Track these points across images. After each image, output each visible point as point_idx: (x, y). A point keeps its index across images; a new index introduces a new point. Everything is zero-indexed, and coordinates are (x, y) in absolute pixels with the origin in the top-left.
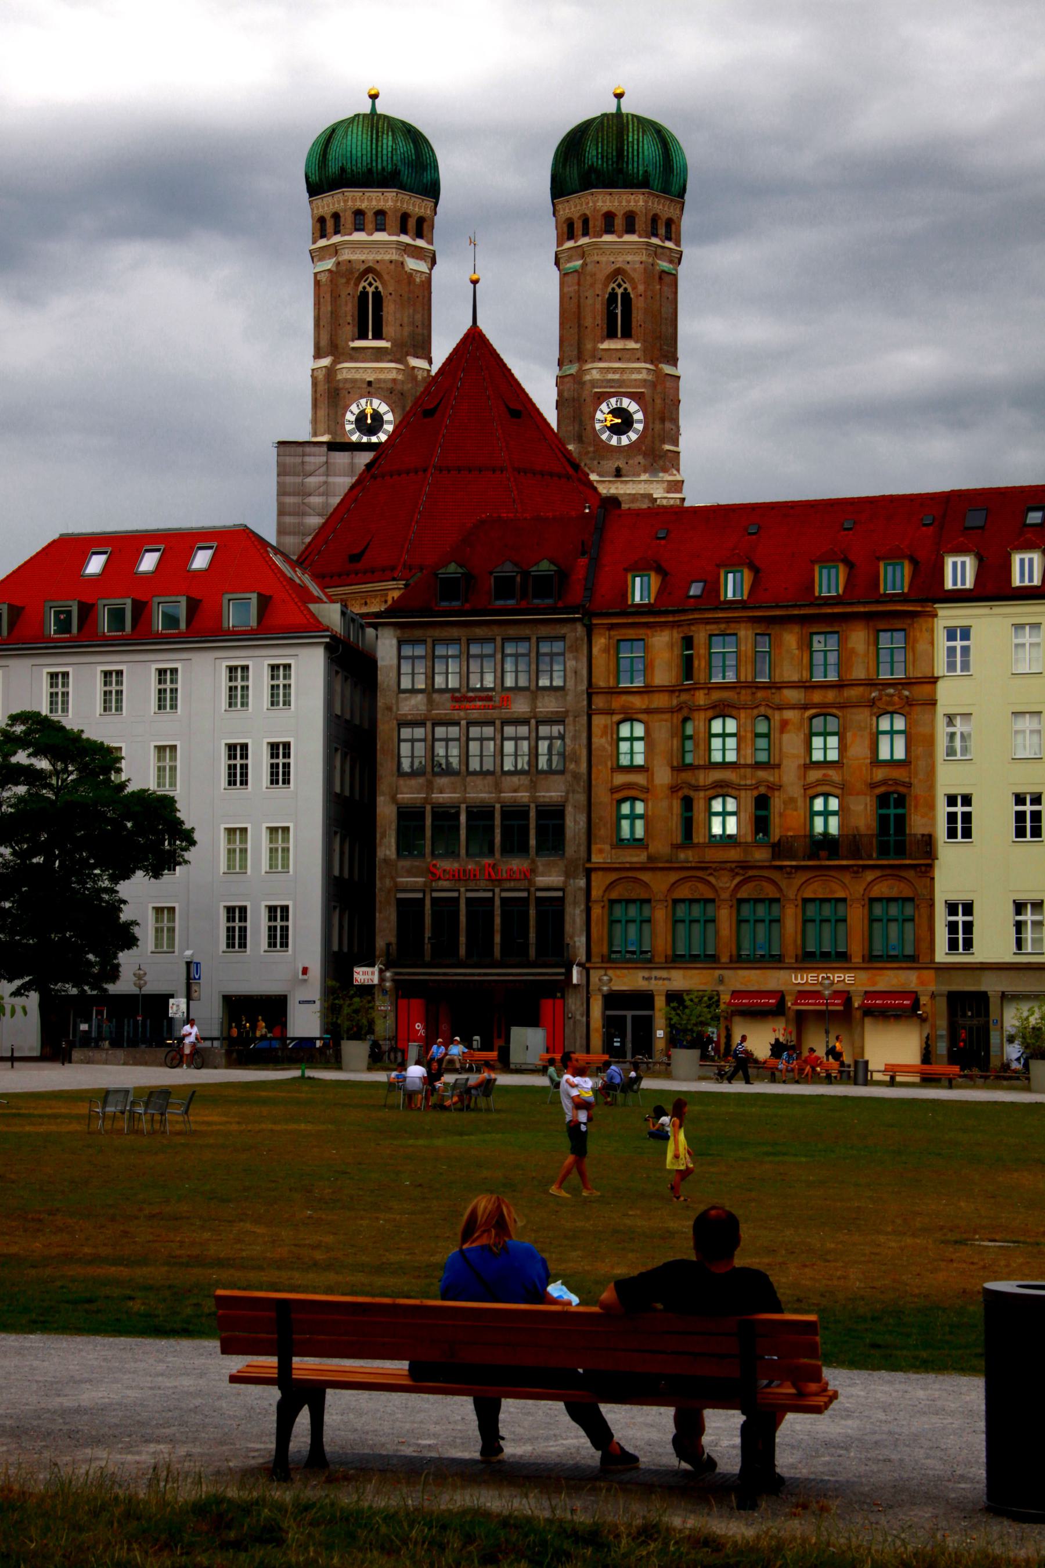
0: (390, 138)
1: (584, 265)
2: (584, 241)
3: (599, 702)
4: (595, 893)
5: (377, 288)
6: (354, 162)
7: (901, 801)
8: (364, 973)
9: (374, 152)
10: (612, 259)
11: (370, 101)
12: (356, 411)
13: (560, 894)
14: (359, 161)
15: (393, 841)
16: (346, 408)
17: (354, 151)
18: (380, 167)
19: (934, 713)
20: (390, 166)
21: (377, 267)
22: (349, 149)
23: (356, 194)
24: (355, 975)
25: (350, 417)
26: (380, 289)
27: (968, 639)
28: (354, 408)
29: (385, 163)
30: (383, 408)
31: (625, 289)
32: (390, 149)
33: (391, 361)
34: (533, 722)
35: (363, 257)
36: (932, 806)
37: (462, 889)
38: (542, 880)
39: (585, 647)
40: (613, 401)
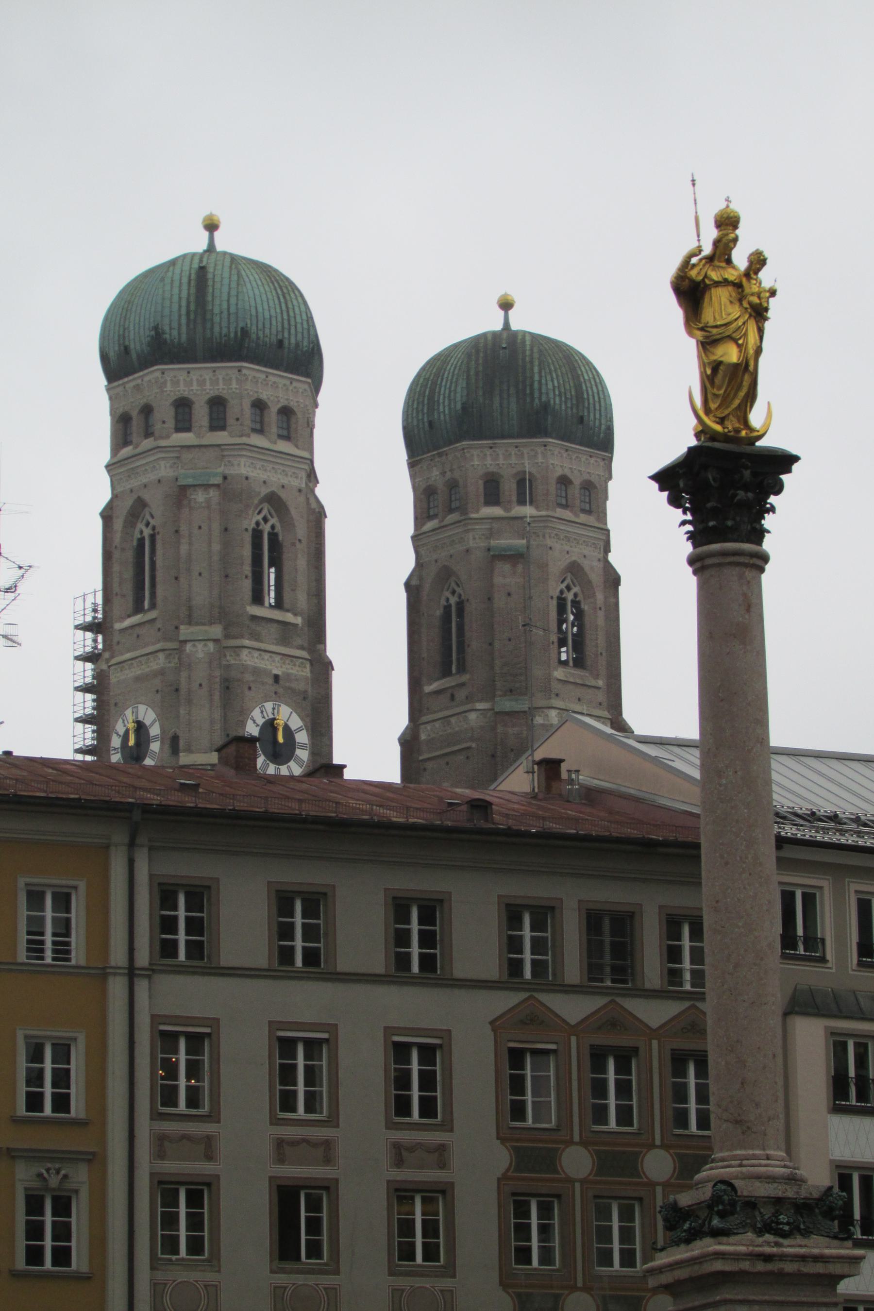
6: (260, 326)
9: (285, 317)
10: (567, 548)
11: (206, 234)
12: (261, 721)
14: (267, 325)
17: (260, 309)
18: (293, 341)
20: (305, 343)
21: (283, 494)
22: (253, 304)
23: (258, 375)
26: (278, 529)
28: (256, 713)
29: (300, 336)
33: (302, 648)
35: (263, 476)
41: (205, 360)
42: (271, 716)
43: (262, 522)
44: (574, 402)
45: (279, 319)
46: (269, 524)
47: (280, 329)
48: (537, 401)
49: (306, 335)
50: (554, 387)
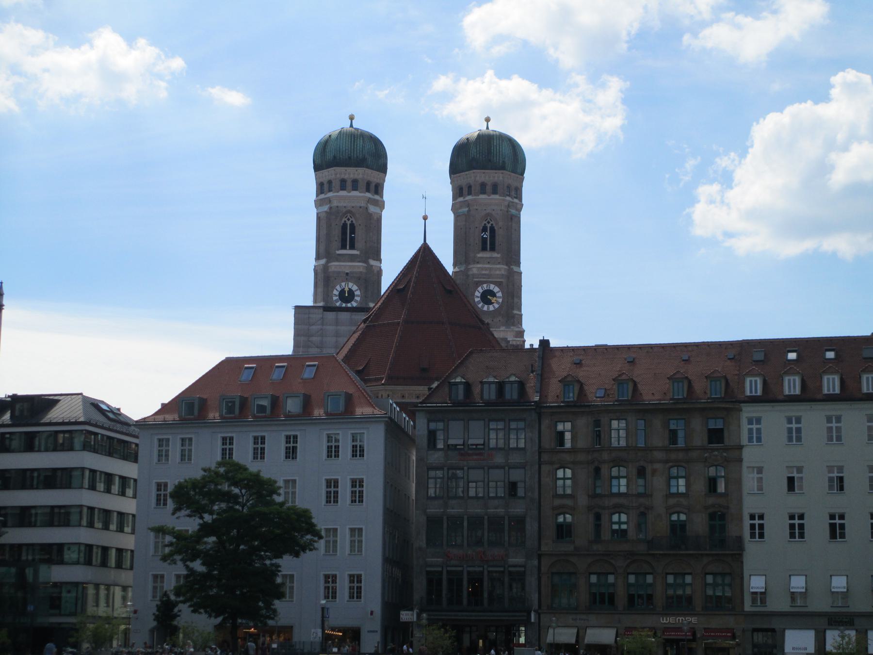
0: (361, 141)
1: (469, 211)
2: (469, 198)
3: (545, 457)
4: (544, 569)
5: (352, 221)
6: (341, 154)
7: (723, 517)
8: (406, 615)
9: (352, 148)
12: (339, 289)
13: (523, 569)
14: (344, 153)
15: (424, 537)
16: (334, 287)
17: (341, 147)
18: (355, 156)
19: (741, 467)
20: (361, 156)
22: (338, 146)
24: (401, 616)
25: (336, 292)
26: (354, 222)
27: (760, 424)
29: (358, 154)
30: (355, 288)
31: (492, 225)
32: (361, 147)
33: (359, 262)
34: (507, 468)
36: (741, 519)
37: (465, 566)
38: (512, 561)
39: (537, 426)
40: (485, 286)
41: (326, 169)
42: (344, 287)
43: (347, 221)
44: (486, 154)
45: (350, 150)
46: (350, 221)
47: (349, 153)
48: (470, 157)
49: (361, 153)
50: (477, 151)
